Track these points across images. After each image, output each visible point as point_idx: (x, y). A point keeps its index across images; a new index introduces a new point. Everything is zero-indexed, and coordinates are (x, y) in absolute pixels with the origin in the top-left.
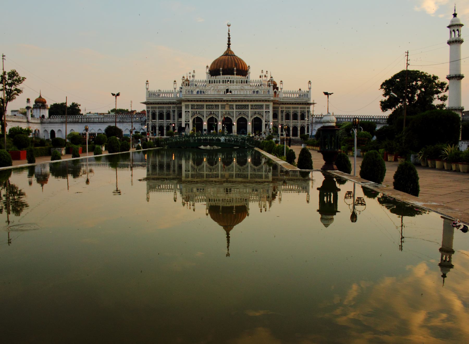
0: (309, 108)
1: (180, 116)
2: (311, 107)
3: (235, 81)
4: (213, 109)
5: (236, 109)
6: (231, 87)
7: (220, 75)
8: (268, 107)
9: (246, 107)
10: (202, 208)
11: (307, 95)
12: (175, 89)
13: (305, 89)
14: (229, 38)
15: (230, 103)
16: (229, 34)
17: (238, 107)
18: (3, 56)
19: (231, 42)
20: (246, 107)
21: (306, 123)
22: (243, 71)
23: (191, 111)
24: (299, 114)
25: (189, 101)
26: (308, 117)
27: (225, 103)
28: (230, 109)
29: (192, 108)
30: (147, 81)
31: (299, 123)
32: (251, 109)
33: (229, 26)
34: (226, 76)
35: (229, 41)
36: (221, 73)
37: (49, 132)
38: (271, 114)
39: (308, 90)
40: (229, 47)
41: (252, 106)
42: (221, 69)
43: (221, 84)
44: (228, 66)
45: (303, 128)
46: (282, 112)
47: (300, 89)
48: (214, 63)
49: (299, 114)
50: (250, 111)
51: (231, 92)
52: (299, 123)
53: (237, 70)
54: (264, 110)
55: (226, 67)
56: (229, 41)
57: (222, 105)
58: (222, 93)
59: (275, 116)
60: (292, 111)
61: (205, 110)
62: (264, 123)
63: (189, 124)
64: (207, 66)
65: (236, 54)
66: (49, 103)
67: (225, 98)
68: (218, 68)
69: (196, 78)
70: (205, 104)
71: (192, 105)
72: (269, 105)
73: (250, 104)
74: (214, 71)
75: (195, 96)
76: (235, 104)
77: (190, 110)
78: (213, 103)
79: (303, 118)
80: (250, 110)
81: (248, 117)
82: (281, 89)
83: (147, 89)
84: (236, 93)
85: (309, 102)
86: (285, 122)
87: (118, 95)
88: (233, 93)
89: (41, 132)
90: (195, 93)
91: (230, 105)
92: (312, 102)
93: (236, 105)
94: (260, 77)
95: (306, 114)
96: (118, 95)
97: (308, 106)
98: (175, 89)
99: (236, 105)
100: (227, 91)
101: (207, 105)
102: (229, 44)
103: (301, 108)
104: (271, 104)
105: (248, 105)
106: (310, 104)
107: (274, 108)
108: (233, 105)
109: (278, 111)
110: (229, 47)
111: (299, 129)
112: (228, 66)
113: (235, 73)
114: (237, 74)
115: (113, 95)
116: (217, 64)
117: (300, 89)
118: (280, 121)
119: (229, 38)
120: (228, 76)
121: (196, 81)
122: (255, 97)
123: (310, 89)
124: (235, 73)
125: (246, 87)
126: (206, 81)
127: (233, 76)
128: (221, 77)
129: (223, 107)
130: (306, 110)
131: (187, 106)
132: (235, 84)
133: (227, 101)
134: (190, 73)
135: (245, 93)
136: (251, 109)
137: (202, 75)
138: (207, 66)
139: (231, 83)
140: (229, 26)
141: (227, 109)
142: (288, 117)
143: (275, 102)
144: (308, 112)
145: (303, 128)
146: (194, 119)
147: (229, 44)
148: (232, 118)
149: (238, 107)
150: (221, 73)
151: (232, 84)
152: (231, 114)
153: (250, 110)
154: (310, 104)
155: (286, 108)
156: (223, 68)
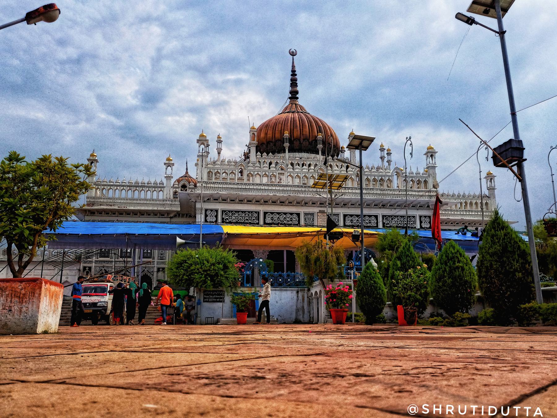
12: (169, 178)
19: (299, 88)
27: (316, 210)
34: (298, 155)
44: (302, 130)
48: (265, 126)
55: (297, 133)
68: (278, 135)
70: (261, 209)
93: (345, 216)
102: (294, 95)
105: (376, 217)
112: (302, 130)
113: (320, 146)
123: (491, 189)
127: (313, 155)
140: (293, 54)
147: (294, 95)
150: (287, 145)
156: (291, 133)
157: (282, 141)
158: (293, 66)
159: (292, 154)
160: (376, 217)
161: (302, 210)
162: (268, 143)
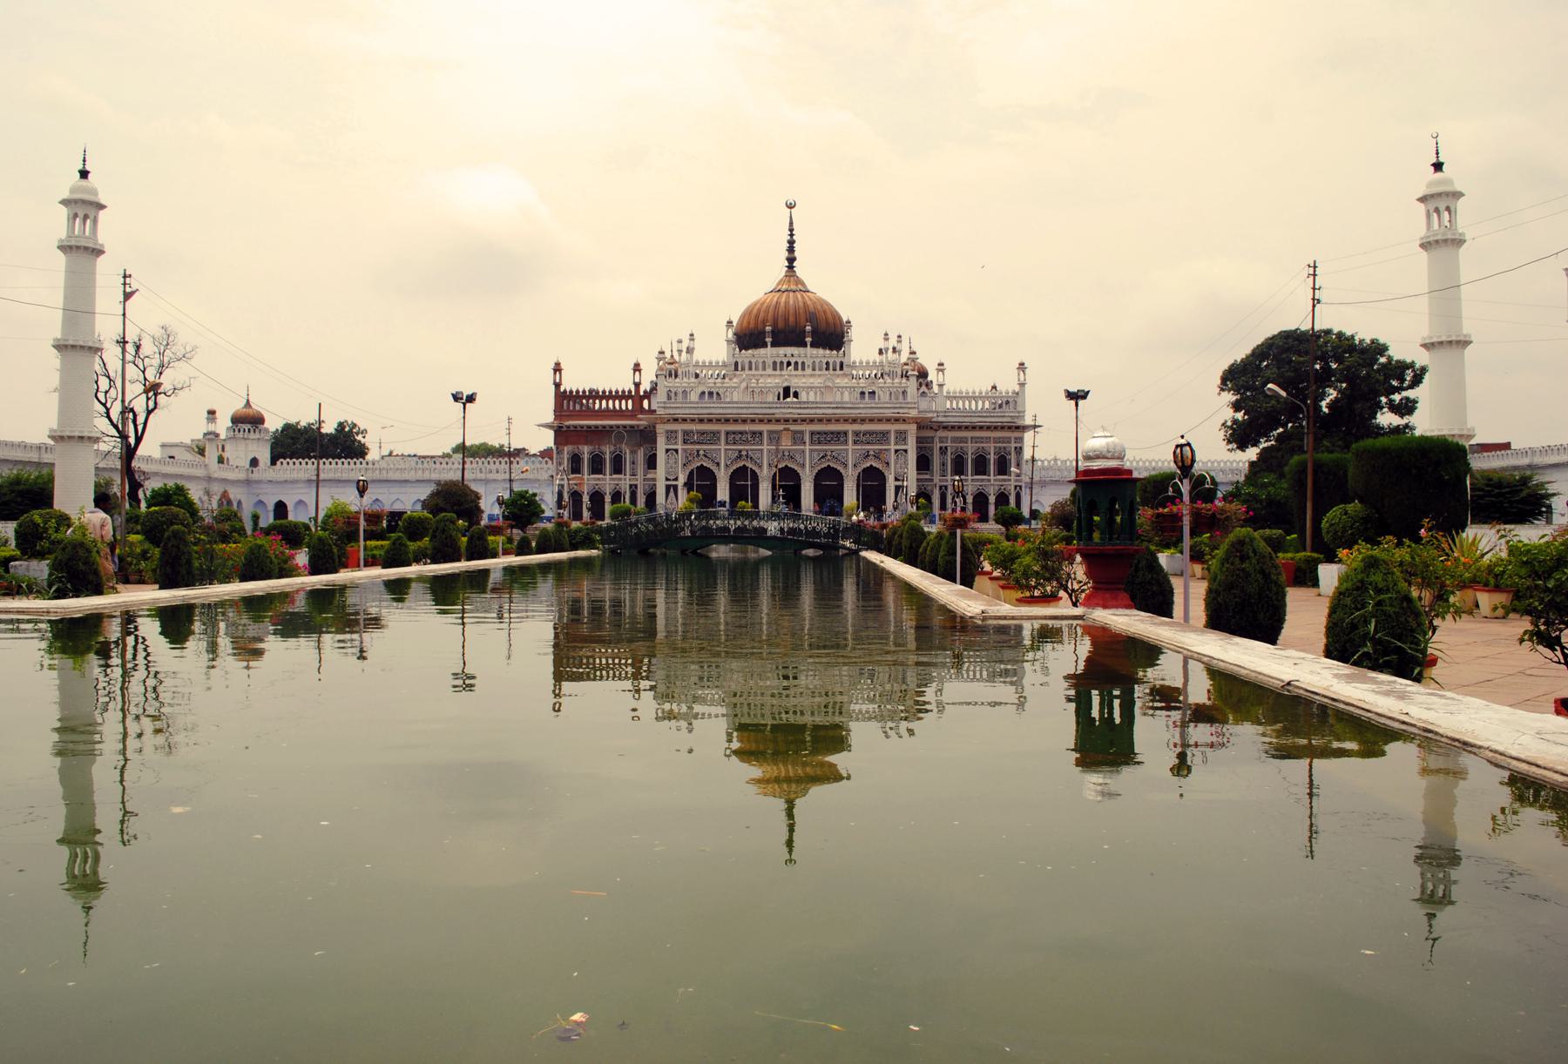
0: (1021, 440)
1: (651, 463)
2: (1028, 436)
3: (808, 362)
4: (747, 442)
5: (812, 443)
6: (797, 381)
7: (764, 345)
8: (902, 437)
9: (839, 437)
10: (713, 728)
11: (1012, 401)
12: (637, 385)
13: (1008, 385)
14: (791, 243)
15: (793, 427)
16: (791, 230)
17: (818, 437)
18: (125, 277)
19: (796, 254)
20: (839, 437)
21: (1013, 483)
22: (829, 333)
23: (685, 451)
24: (992, 458)
25: (676, 420)
26: (1018, 465)
27: (781, 427)
28: (795, 443)
29: (685, 442)
30: (558, 364)
31: (992, 484)
32: (855, 443)
33: (791, 206)
34: (782, 350)
35: (791, 249)
36: (769, 340)
37: (271, 507)
38: (912, 457)
39: (1017, 388)
40: (791, 267)
41: (856, 434)
42: (768, 328)
43: (769, 371)
45: (1002, 498)
46: (943, 451)
47: (994, 387)
49: (992, 458)
50: (851, 451)
51: (796, 395)
52: (992, 484)
53: (814, 333)
54: (893, 447)
55: (781, 325)
56: (791, 249)
57: (770, 432)
58: (771, 398)
59: (923, 463)
60: (970, 450)
61: (723, 447)
62: (891, 485)
63: (675, 487)
64: (730, 322)
65: (810, 288)
66: (273, 424)
67: (780, 413)
69: (700, 355)
70: (723, 428)
71: (686, 433)
72: (905, 432)
73: (850, 428)
74: (748, 337)
75: (693, 404)
76: (808, 428)
77: (679, 447)
78: (743, 429)
79: (1003, 468)
80: (850, 446)
81: (846, 466)
82: (941, 386)
83: (557, 385)
84: (812, 398)
85: (1020, 423)
86: (951, 479)
87: (471, 399)
88: (803, 397)
89: (244, 505)
90: (694, 397)
91: (795, 432)
92: (1028, 421)
93: (812, 433)
94: (881, 352)
95: (1013, 457)
96: (471, 399)
97: (1016, 434)
98: (637, 385)
99: (812, 433)
100: (787, 391)
101: (727, 433)
102: (791, 260)
103: (996, 440)
104: (912, 429)
105: (845, 433)
106: (1025, 428)
107: (919, 440)
108: (802, 432)
109: (931, 449)
110: (791, 267)
111: (992, 499)
112: (786, 320)
113: (809, 340)
114: (813, 345)
115: (456, 397)
116: (757, 316)
117: (994, 387)
118: (937, 478)
119: (791, 243)
120: (789, 350)
121: (697, 365)
122: (866, 408)
123: (1022, 385)
124: (809, 340)
125: (844, 382)
126: (725, 365)
127: (802, 350)
128: (769, 353)
129: (775, 438)
130: (1013, 445)
131: (671, 435)
132: (808, 371)
133: (787, 421)
134: (680, 342)
135: (838, 399)
136: (855, 443)
137: (715, 348)
138: (730, 322)
139: (796, 369)
140: (791, 206)
141: (786, 444)
142: (959, 468)
143: (923, 425)
144: (1019, 451)
145: (1002, 498)
146: (691, 473)
147: (791, 260)
148: (799, 470)
149: (818, 437)
150: (769, 340)
151: (800, 372)
152: (798, 457)
153: (850, 446)
154: (1025, 428)
155: (955, 440)
156: (775, 325)
157: (762, 333)
158: (791, 223)
159: (775, 350)
160: (845, 433)
161: (764, 428)
162: (751, 334)
